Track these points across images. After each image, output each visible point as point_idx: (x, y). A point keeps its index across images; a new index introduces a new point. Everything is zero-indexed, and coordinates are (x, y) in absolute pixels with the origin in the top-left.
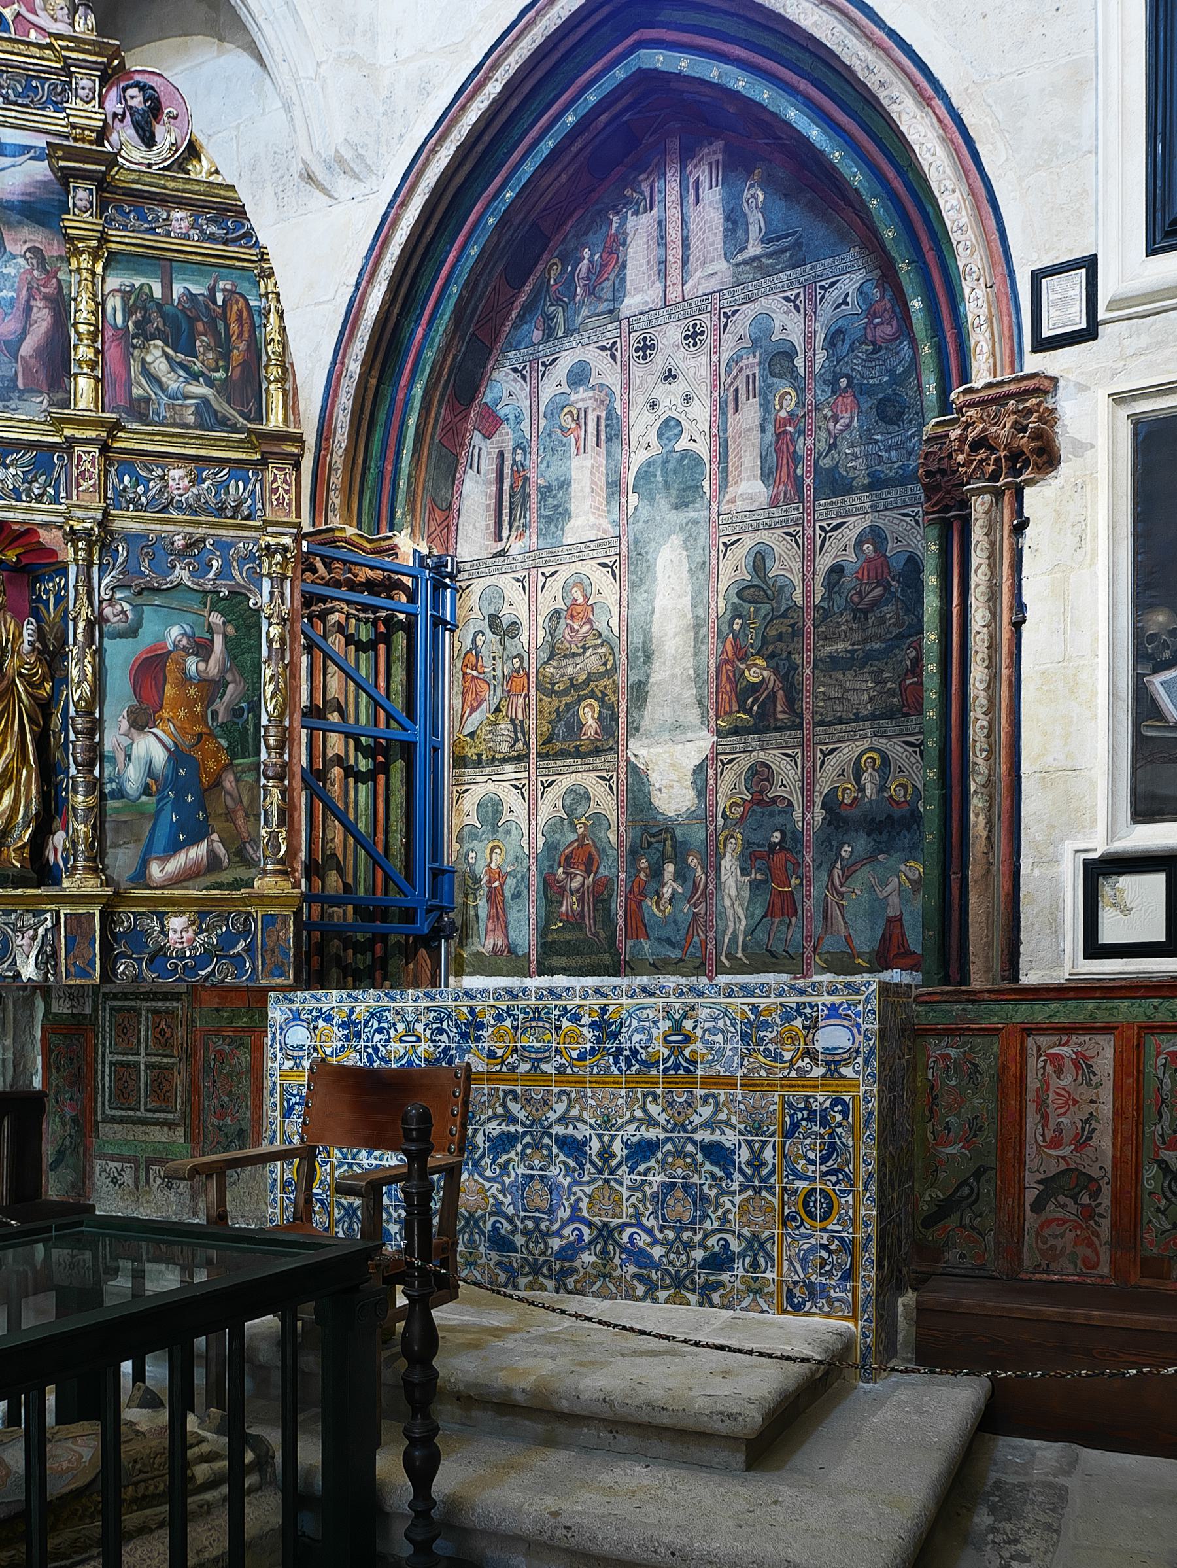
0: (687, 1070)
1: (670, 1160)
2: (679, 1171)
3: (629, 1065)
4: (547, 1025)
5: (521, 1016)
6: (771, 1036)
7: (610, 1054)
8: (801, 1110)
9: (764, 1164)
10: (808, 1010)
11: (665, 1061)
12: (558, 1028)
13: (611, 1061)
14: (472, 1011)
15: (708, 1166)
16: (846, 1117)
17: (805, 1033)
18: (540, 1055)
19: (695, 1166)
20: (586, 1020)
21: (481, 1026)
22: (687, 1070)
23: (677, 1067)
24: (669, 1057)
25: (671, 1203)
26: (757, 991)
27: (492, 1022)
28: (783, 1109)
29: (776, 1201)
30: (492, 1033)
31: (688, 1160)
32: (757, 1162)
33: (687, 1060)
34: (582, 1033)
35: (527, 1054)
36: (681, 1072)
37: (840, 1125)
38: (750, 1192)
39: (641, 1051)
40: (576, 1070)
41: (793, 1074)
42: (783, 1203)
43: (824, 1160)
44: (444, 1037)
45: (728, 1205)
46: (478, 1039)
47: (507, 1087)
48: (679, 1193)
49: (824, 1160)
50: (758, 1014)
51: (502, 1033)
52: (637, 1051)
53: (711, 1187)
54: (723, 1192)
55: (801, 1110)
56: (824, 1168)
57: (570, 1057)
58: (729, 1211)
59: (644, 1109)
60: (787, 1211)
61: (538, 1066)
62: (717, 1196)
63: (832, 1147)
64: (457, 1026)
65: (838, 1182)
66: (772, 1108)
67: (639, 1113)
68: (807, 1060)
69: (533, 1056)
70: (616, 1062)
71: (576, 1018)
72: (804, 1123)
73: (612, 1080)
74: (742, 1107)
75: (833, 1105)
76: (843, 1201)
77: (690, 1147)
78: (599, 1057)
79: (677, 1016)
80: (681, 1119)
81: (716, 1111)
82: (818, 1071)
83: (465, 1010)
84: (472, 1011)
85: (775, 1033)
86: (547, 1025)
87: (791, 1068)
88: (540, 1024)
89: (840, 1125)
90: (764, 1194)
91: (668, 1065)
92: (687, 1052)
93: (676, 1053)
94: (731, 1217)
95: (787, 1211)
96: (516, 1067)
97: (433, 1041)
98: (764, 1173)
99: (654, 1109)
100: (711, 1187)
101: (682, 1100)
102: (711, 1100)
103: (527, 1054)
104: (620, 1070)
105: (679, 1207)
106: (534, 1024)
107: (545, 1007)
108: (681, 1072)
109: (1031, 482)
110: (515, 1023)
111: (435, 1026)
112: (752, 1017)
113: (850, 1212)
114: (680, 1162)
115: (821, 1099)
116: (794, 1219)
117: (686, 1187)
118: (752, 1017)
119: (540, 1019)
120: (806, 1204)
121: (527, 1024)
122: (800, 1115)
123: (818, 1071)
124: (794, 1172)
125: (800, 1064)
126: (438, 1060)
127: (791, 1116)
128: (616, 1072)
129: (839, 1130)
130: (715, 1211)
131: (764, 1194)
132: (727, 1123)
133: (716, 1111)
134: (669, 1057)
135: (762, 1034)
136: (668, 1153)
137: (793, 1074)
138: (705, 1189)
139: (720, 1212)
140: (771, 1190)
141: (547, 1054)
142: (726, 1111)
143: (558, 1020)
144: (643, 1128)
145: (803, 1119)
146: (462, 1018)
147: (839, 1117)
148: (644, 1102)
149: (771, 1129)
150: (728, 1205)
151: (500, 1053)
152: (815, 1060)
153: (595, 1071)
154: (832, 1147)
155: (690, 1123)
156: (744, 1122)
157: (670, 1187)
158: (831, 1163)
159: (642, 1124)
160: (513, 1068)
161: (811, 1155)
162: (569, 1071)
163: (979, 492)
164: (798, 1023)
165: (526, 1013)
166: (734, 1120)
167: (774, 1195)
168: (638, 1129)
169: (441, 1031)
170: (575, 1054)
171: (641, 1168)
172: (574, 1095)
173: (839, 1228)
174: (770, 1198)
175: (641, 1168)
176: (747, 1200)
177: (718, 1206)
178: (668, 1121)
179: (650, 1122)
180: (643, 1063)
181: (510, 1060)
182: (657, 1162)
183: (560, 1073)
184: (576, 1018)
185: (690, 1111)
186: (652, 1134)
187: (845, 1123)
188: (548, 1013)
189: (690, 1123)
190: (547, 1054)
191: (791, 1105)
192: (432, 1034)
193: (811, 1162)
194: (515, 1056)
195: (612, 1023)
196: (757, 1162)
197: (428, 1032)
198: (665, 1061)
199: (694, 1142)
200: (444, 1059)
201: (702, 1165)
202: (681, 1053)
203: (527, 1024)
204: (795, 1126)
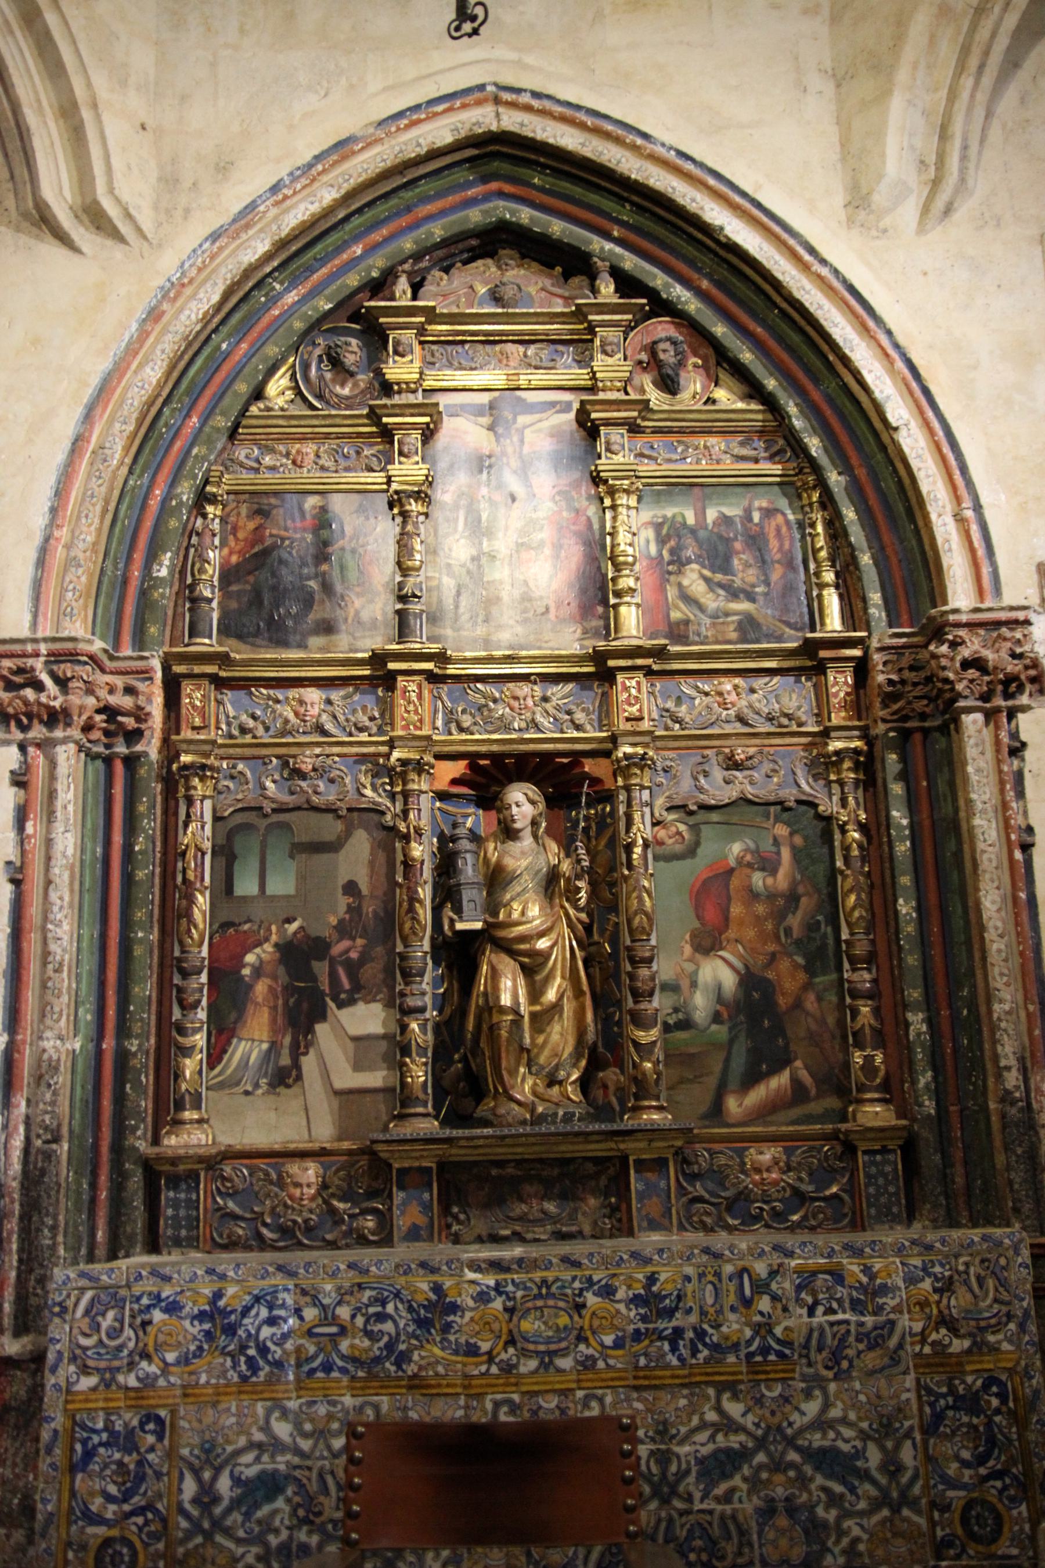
0: (781, 1355)
1: (764, 1475)
2: (780, 1490)
3: (695, 1352)
4: (561, 1304)
5: (519, 1294)
6: (893, 1303)
7: (661, 1338)
8: (944, 1396)
9: (900, 1468)
10: (937, 1269)
11: (749, 1342)
12: (580, 1307)
13: (666, 1347)
14: (437, 1288)
15: (820, 1480)
16: (1004, 1400)
17: (936, 1297)
18: (553, 1347)
19: (803, 1481)
20: (621, 1294)
21: (454, 1308)
22: (781, 1355)
23: (765, 1350)
24: (753, 1338)
25: (771, 1535)
26: (867, 1250)
27: (471, 1303)
28: (919, 1397)
29: (922, 1521)
30: (472, 1319)
31: (792, 1474)
32: (892, 1467)
33: (779, 1341)
34: (618, 1312)
35: (531, 1347)
36: (772, 1357)
37: (998, 1411)
38: (885, 1512)
39: (710, 1331)
40: (611, 1362)
41: (927, 1350)
42: (933, 1524)
43: (981, 1460)
44: (388, 1327)
45: (856, 1531)
46: (447, 1328)
47: (499, 1397)
48: (783, 1521)
49: (981, 1460)
50: (872, 1277)
51: (489, 1318)
52: (704, 1333)
53: (827, 1509)
54: (846, 1514)
55: (944, 1396)
56: (983, 1471)
57: (602, 1345)
58: (856, 1540)
59: (718, 1409)
60: (939, 1533)
61: (551, 1362)
62: (839, 1520)
63: (992, 1442)
64: (410, 1309)
65: (1005, 1488)
66: (904, 1396)
67: (712, 1416)
68: (943, 1331)
69: (542, 1348)
70: (674, 1349)
71: (608, 1292)
72: (950, 1413)
73: (668, 1373)
74: (862, 1398)
75: (986, 1387)
76: (1015, 1512)
77: (793, 1456)
78: (646, 1342)
79: (774, 1286)
80: (775, 1420)
81: (826, 1406)
82: (958, 1345)
83: (425, 1286)
84: (437, 1288)
85: (897, 1300)
86: (561, 1304)
87: (923, 1341)
88: (551, 1302)
89: (998, 1411)
90: (906, 1512)
91: (753, 1348)
92: (778, 1331)
93: (763, 1332)
94: (861, 1547)
95: (939, 1533)
96: (516, 1366)
97: (368, 1334)
98: (904, 1480)
99: (734, 1409)
100: (827, 1509)
101: (776, 1394)
102: (817, 1392)
103: (531, 1347)
104: (681, 1359)
105: (783, 1542)
106: (540, 1303)
107: (557, 1279)
108: (772, 1357)
109: (1024, 709)
110: (510, 1304)
111: (372, 1310)
112: (865, 1280)
113: (1027, 1527)
114: (779, 1478)
115: (969, 1379)
116: (950, 1545)
117: (792, 1511)
118: (865, 1280)
119: (550, 1295)
120: (965, 1521)
121: (530, 1305)
122: (942, 1402)
123: (958, 1345)
124: (945, 1479)
125: (934, 1336)
126: (377, 1360)
127: (932, 1405)
128: (675, 1362)
129: (997, 1419)
130: (837, 1542)
131: (906, 1512)
132: (844, 1421)
133: (826, 1406)
134: (753, 1338)
135: (881, 1301)
136: (761, 1467)
137: (927, 1350)
138: (820, 1511)
139: (845, 1541)
140: (913, 1504)
141: (564, 1344)
142: (839, 1404)
143: (580, 1295)
144: (720, 1437)
145: (948, 1407)
146: (420, 1298)
147: (995, 1402)
148: (718, 1400)
149: (907, 1424)
150: (856, 1531)
151: (485, 1347)
152: (954, 1331)
153: (642, 1361)
154: (992, 1442)
155: (790, 1424)
156: (867, 1418)
157: (768, 1511)
158: (991, 1463)
159: (717, 1431)
160: (508, 1368)
161: (966, 1455)
162: (601, 1364)
163: (969, 710)
164: (927, 1285)
165: (526, 1288)
166: (852, 1416)
167: (919, 1512)
168: (712, 1438)
169: (382, 1317)
170: (608, 1340)
171: (720, 1490)
172: (608, 1399)
173: (1015, 1551)
174: (916, 1518)
175: (720, 1490)
176: (883, 1522)
177: (841, 1533)
178: (757, 1425)
179: (728, 1425)
180: (715, 1347)
181: (504, 1356)
182: (745, 1479)
183: (586, 1368)
184: (608, 1292)
185: (788, 1408)
186: (735, 1441)
187: (1004, 1409)
188: (563, 1287)
189: (790, 1424)
190: (564, 1344)
191: (930, 1391)
192: (367, 1322)
193: (965, 1464)
194: (511, 1350)
195: (665, 1297)
196: (892, 1467)
197: (360, 1321)
198: (749, 1342)
199: (799, 1449)
200: (388, 1357)
201: (812, 1479)
202: (770, 1332)
203: (530, 1305)
204: (938, 1417)
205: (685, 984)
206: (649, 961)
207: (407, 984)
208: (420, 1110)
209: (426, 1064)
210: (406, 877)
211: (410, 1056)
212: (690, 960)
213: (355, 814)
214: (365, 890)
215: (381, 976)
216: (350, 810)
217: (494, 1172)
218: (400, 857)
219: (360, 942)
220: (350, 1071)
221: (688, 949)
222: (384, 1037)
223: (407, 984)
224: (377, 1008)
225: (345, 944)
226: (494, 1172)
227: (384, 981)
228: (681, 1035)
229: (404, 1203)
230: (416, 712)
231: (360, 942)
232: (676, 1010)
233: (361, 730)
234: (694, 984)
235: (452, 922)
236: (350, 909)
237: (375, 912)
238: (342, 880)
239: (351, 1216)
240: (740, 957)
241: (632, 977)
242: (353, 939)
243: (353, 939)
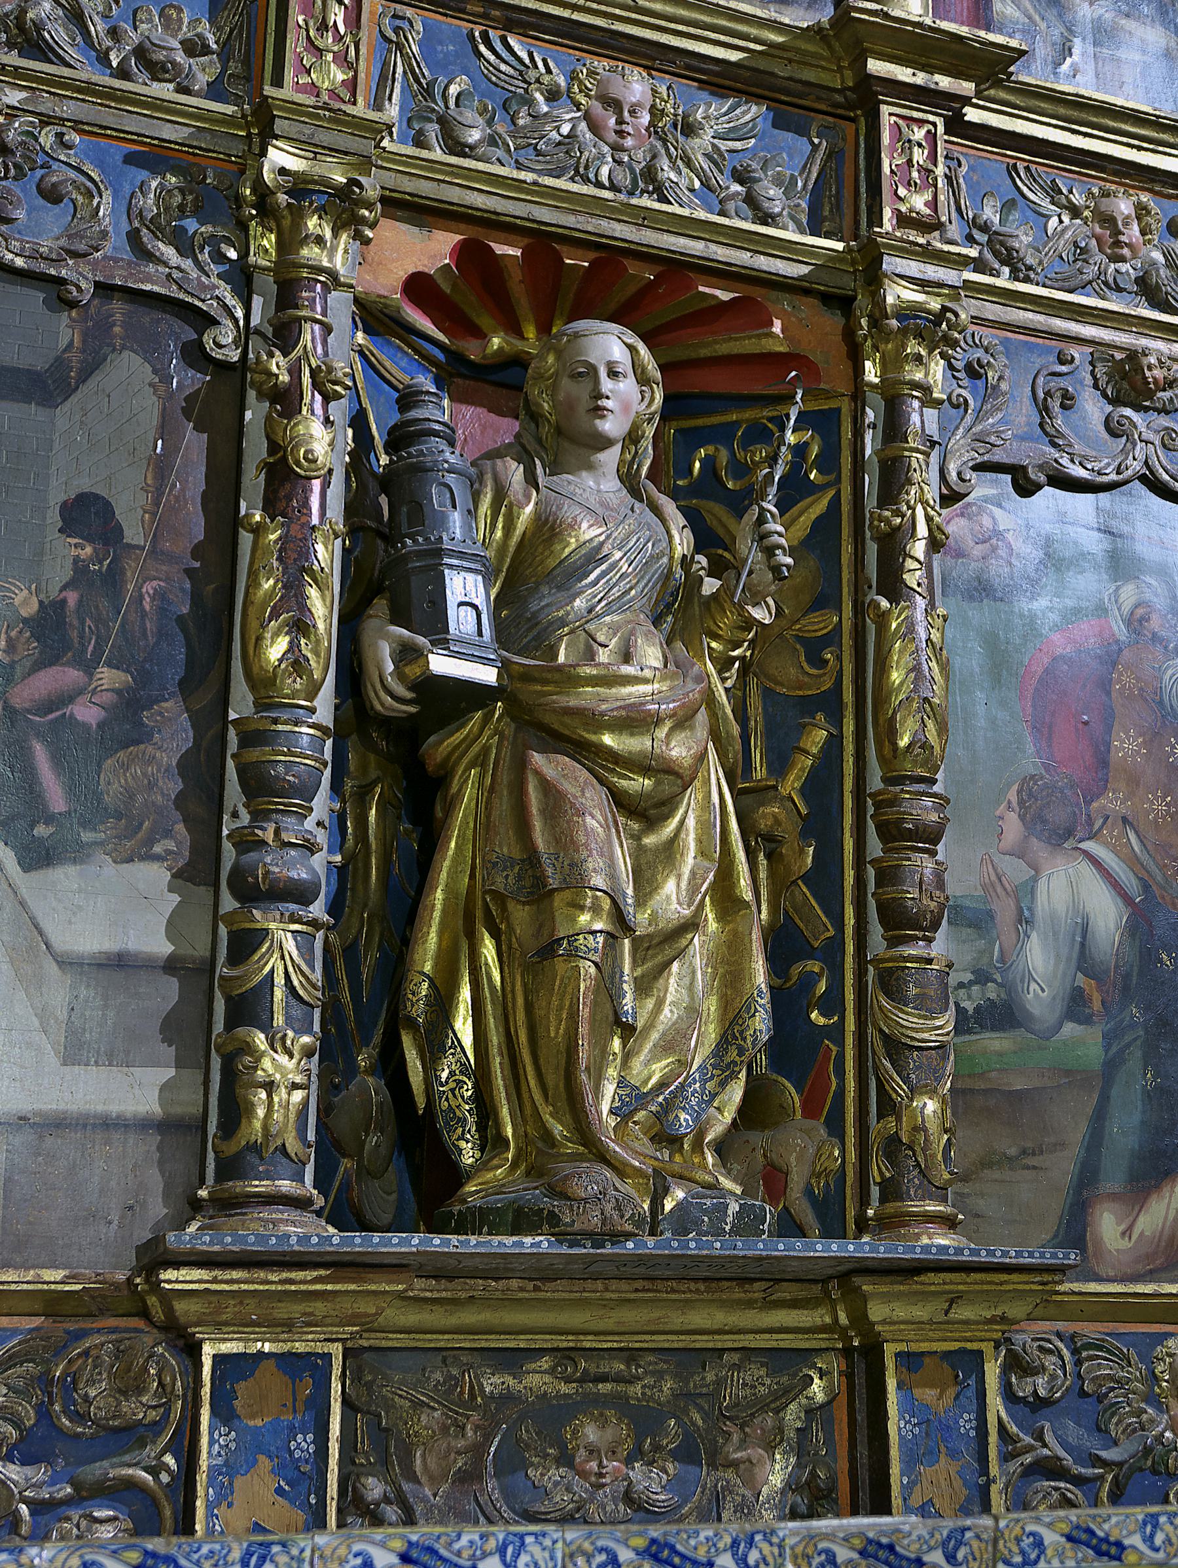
205: (1004, 911)
206: (931, 836)
207: (259, 816)
208: (285, 1185)
209: (308, 1053)
210: (271, 506)
211: (266, 1026)
212: (1020, 853)
213: (118, 308)
214: (134, 534)
215: (174, 786)
216: (103, 289)
217: (492, 1383)
218: (256, 449)
219: (109, 677)
220: (52, 1060)
221: (1013, 826)
222: (171, 966)
223: (259, 816)
224: (155, 875)
225: (68, 676)
226: (492, 1383)
227: (180, 801)
228: (995, 1042)
229: (228, 1469)
230: (342, 60)
231: (109, 677)
232: (982, 977)
233: (157, 71)
234: (1024, 920)
235: (407, 654)
236: (80, 573)
237: (160, 595)
238: (57, 495)
239: (37, 1507)
240: (1132, 861)
241: (888, 876)
242: (89, 668)
243: (89, 668)
